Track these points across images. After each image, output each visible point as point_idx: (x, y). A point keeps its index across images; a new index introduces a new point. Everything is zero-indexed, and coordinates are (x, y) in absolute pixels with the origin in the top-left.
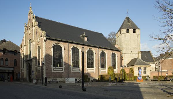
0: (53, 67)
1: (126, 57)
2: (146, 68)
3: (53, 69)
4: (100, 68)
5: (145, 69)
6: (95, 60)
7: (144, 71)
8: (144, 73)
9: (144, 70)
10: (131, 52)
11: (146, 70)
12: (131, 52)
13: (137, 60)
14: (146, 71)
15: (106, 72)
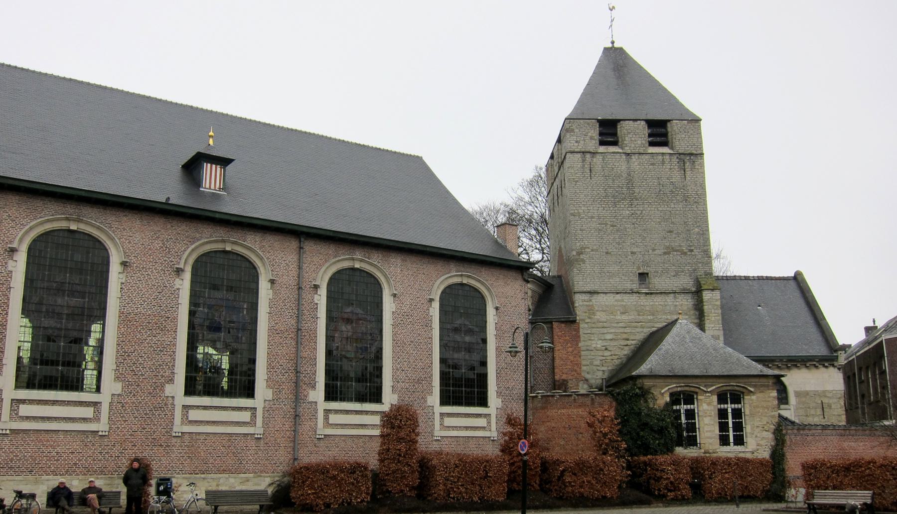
0: (323, 405)
1: (600, 316)
2: (737, 398)
3: (321, 415)
4: (318, 394)
5: (730, 407)
6: (272, 331)
7: (723, 427)
8: (724, 441)
9: (722, 414)
10: (643, 276)
11: (737, 414)
12: (643, 276)
13: (669, 339)
14: (738, 427)
15: (494, 434)
